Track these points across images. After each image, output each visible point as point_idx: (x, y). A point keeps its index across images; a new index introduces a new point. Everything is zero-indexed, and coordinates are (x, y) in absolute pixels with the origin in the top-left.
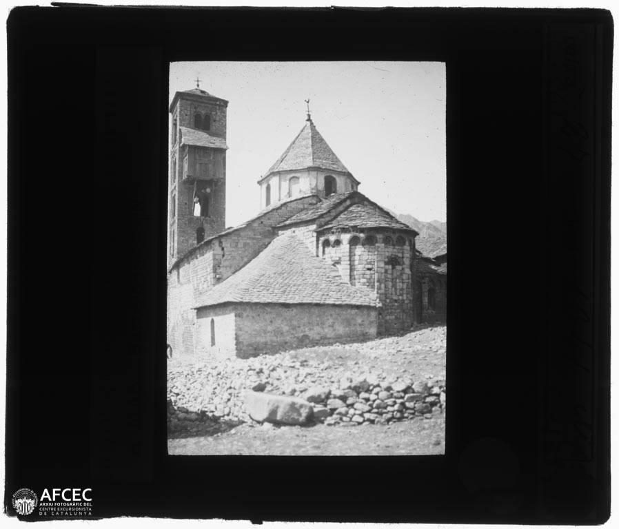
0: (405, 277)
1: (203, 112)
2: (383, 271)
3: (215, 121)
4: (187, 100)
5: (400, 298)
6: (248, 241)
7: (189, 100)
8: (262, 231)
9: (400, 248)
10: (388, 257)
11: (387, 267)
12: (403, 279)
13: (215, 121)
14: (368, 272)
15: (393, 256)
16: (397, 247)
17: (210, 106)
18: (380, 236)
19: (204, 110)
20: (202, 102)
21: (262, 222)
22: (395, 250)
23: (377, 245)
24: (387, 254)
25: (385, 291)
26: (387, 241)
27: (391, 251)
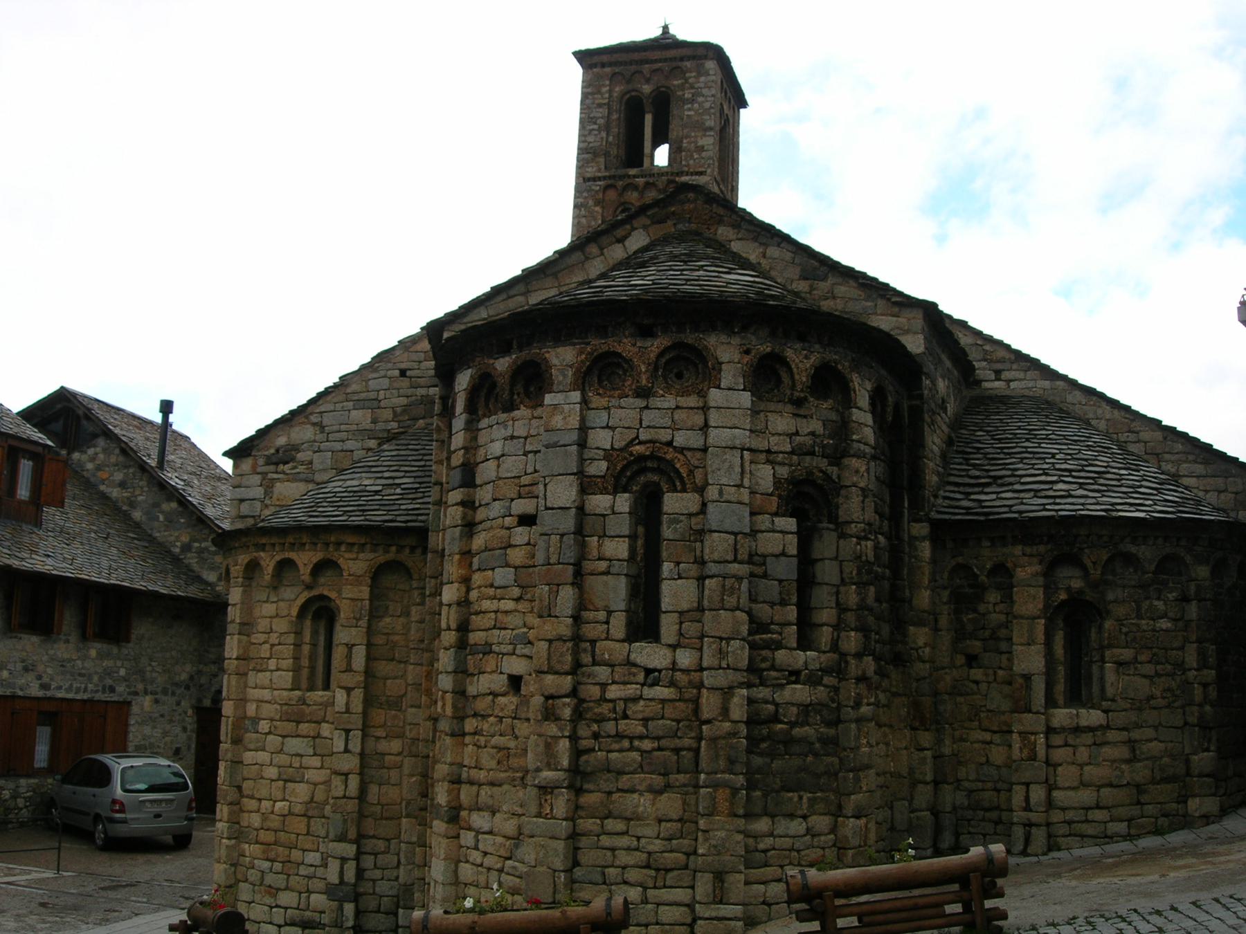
0: (717, 545)
1: (647, 89)
2: (568, 522)
3: (685, 101)
4: (603, 65)
5: (685, 658)
6: (350, 445)
7: (610, 64)
8: (404, 401)
9: (692, 401)
10: (608, 455)
11: (599, 502)
12: (701, 562)
13: (685, 101)
14: (521, 535)
15: (638, 449)
16: (669, 401)
17: (666, 67)
18: (563, 358)
19: (648, 81)
20: (647, 62)
21: (403, 373)
22: (648, 417)
23: (549, 399)
24: (601, 439)
25: (577, 619)
26: (602, 373)
27: (619, 421)
